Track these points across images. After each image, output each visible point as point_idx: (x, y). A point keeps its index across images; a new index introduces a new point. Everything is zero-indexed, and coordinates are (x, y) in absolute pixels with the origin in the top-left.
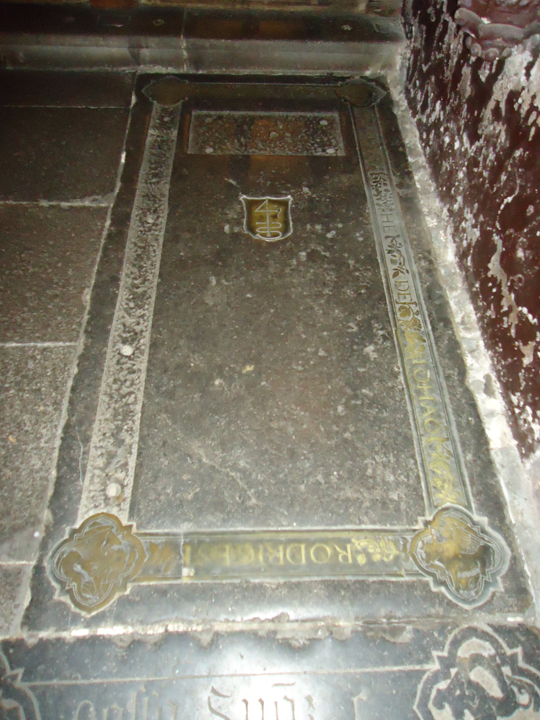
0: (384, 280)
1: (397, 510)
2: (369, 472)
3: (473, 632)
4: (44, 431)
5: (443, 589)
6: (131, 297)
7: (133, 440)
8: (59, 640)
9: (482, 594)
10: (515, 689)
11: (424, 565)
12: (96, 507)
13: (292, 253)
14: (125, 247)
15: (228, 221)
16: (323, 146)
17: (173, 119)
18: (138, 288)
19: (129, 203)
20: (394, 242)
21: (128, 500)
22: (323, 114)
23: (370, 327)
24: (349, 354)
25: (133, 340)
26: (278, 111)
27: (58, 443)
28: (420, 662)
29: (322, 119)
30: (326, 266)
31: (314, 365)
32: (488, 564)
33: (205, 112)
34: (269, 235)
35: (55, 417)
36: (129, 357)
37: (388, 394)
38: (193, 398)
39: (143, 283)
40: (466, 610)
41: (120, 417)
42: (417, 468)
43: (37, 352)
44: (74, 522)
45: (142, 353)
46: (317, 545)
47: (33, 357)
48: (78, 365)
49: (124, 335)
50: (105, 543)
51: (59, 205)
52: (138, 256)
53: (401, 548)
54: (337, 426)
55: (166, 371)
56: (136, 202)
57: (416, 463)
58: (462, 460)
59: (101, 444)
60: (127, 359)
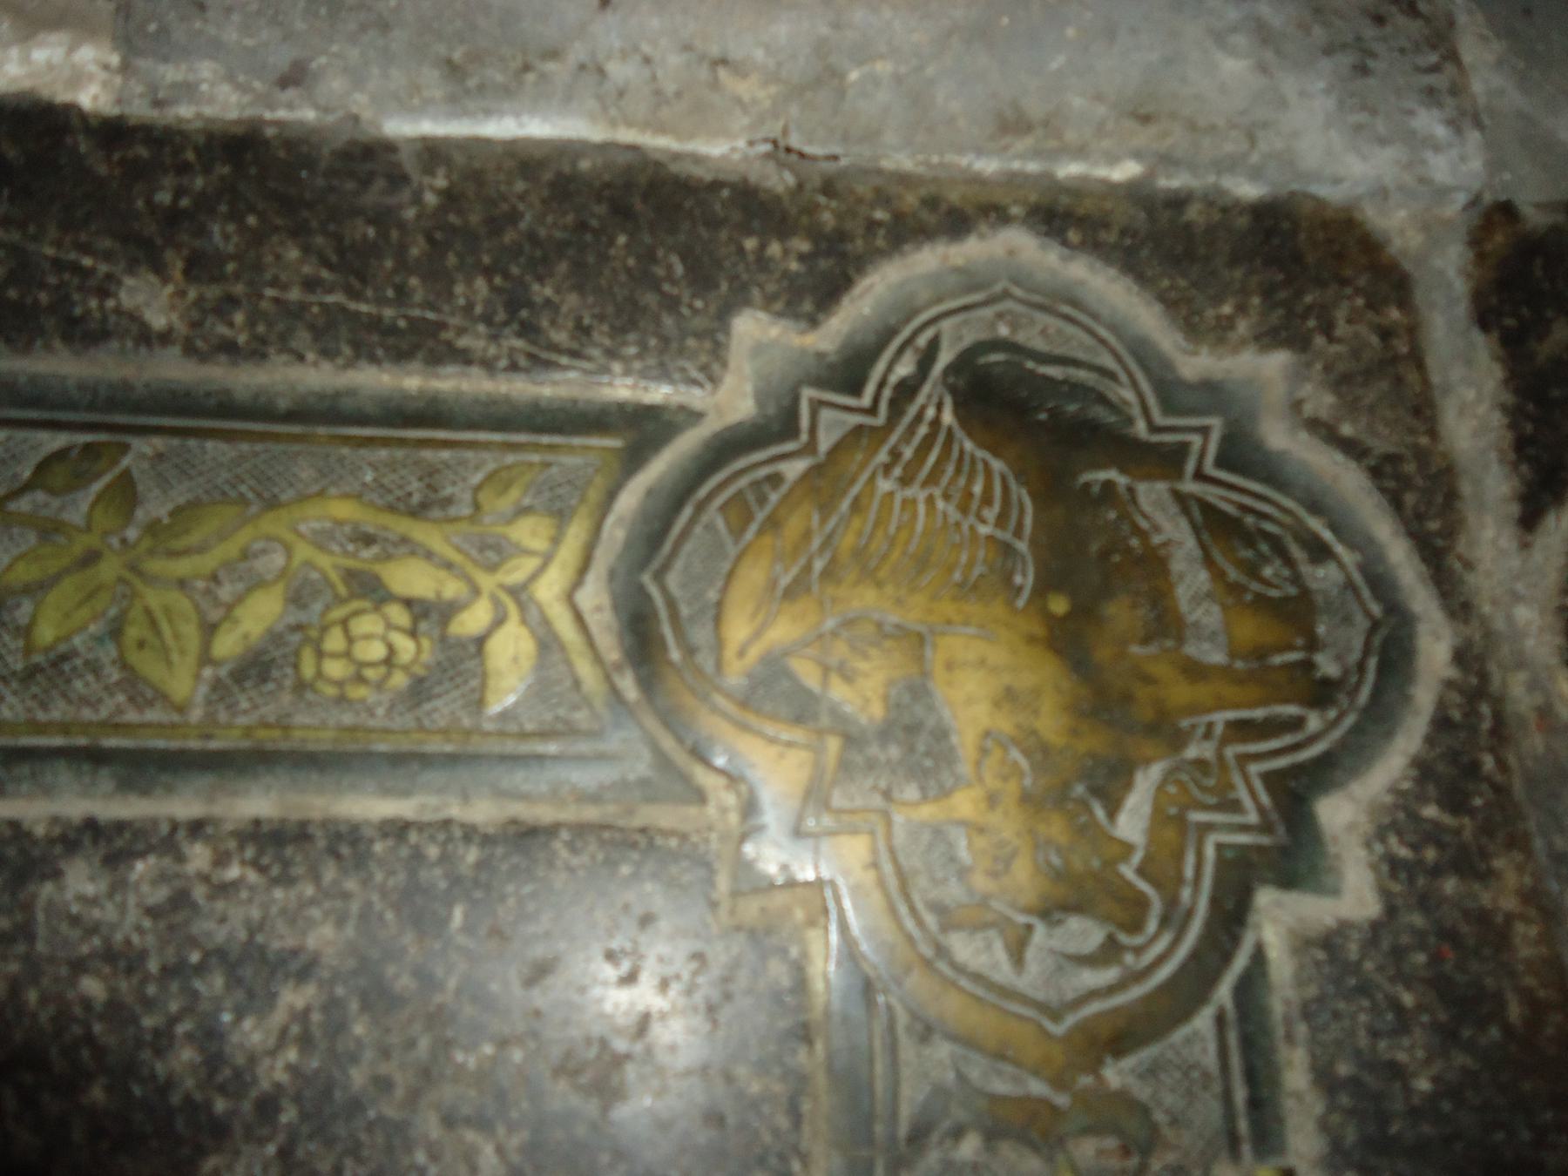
5: (1340, 814)
9: (1315, 508)
11: (1164, 953)
32: (1099, 412)
40: (1461, 657)
57: (113, 844)
58: (173, 369)
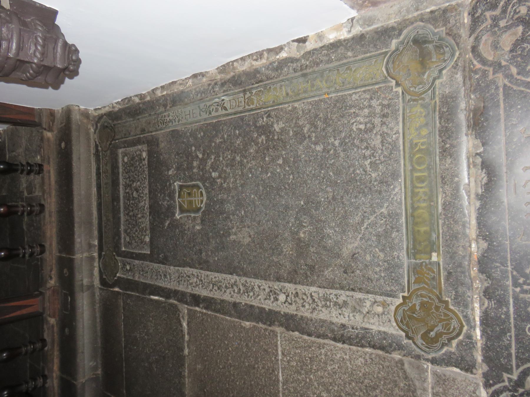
0: (230, 117)
1: (389, 106)
2: (362, 127)
3: (474, 49)
4: (339, 356)
6: (246, 294)
7: (344, 296)
8: (483, 349)
10: (516, 16)
11: (427, 87)
12: (390, 321)
13: (213, 181)
14: (213, 298)
15: (194, 227)
16: (141, 160)
17: (128, 263)
18: (240, 289)
19: (183, 294)
20: (204, 110)
21: (385, 298)
22: (120, 160)
23: (262, 127)
24: (280, 142)
25: (275, 293)
26: (119, 191)
27: (346, 346)
28: (497, 88)
29: (123, 160)
30: (221, 159)
31: (289, 167)
33: (122, 241)
34: (202, 198)
35: (328, 348)
36: (287, 296)
37: (307, 114)
38: (313, 252)
39: (237, 286)
41: (328, 303)
42: (358, 92)
43: (285, 359)
44: (401, 337)
45: (284, 287)
46: (414, 164)
47: (289, 362)
48: (293, 331)
49: (272, 299)
50: (414, 315)
51: (187, 342)
52: (219, 289)
53: (415, 103)
54: (331, 150)
55: (295, 271)
56: (183, 290)
57: (355, 93)
59: (346, 316)
60: (288, 298)
